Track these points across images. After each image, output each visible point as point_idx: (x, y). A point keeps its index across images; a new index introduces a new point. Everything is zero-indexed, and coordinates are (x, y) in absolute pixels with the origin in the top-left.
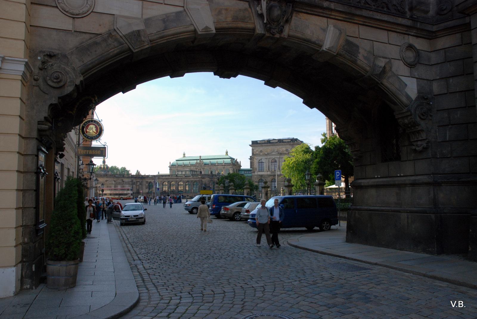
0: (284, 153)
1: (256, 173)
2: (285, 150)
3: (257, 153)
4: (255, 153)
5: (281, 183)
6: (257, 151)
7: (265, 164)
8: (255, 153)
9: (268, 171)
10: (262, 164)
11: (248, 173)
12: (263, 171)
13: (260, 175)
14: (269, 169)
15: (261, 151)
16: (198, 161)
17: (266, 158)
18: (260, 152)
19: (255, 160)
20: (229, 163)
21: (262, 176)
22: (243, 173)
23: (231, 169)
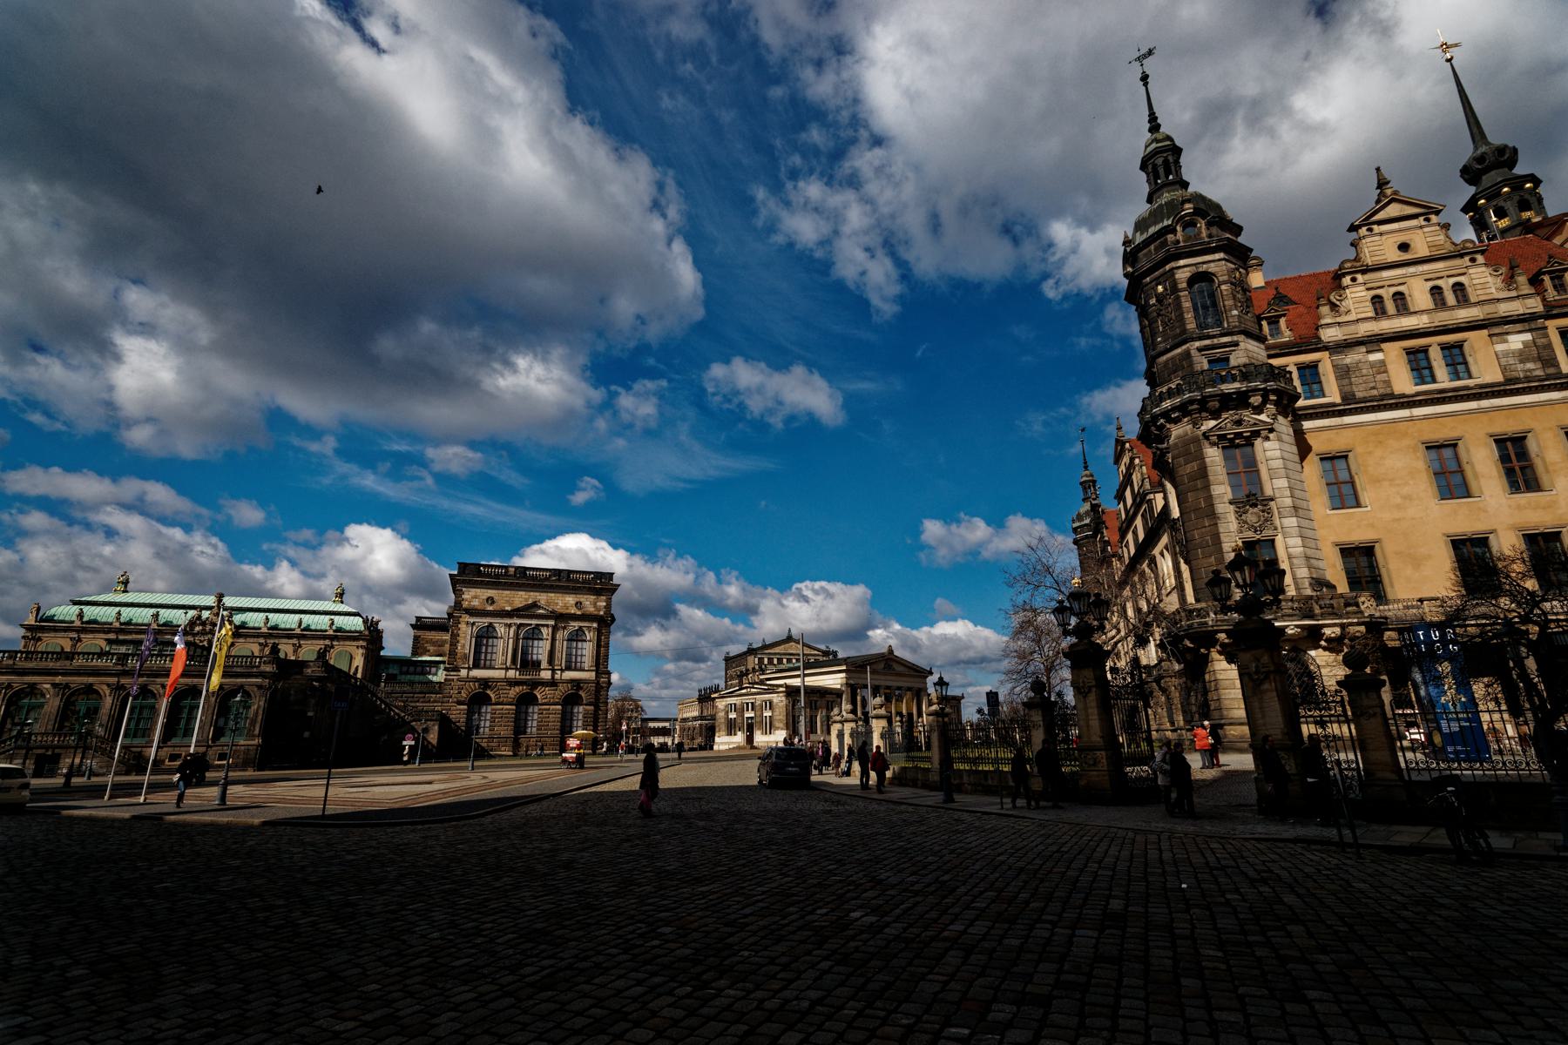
0: (568, 611)
1: (463, 673)
2: (574, 602)
3: (476, 603)
4: (465, 604)
5: (552, 707)
6: (476, 597)
7: (500, 643)
8: (465, 604)
9: (507, 669)
10: (490, 644)
11: (415, 673)
12: (492, 668)
13: (476, 680)
14: (514, 661)
15: (491, 600)
16: (206, 614)
17: (510, 626)
18: (487, 600)
19: (463, 626)
20: (356, 632)
21: (485, 683)
22: (394, 670)
23: (361, 651)
